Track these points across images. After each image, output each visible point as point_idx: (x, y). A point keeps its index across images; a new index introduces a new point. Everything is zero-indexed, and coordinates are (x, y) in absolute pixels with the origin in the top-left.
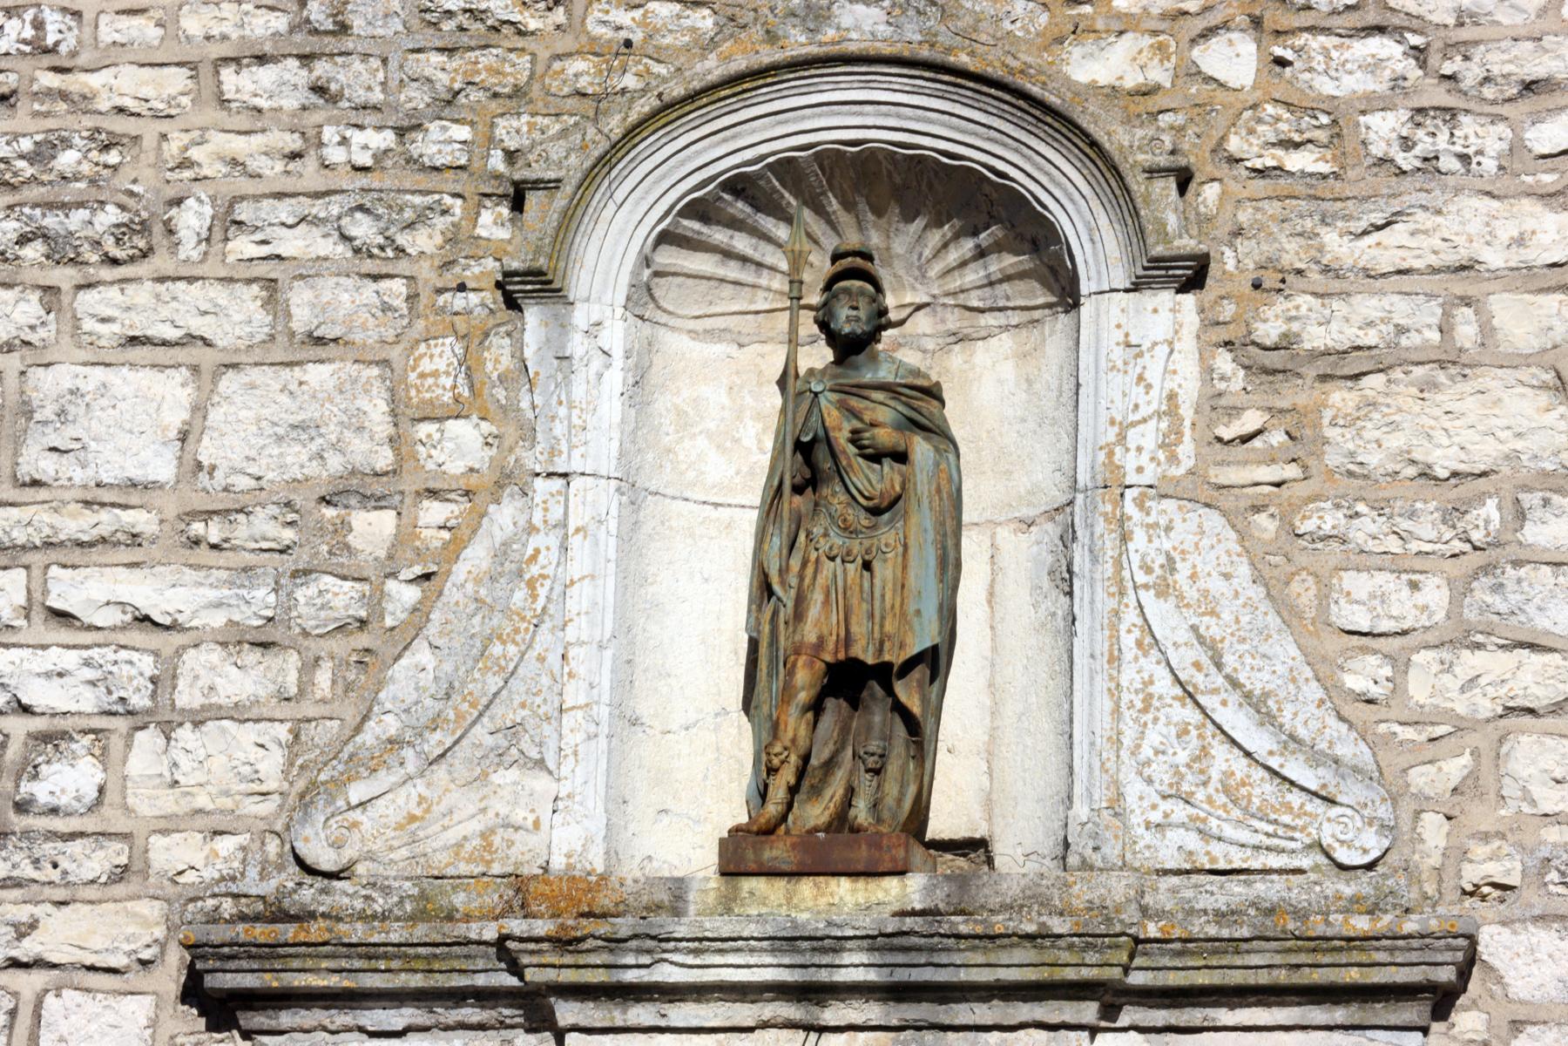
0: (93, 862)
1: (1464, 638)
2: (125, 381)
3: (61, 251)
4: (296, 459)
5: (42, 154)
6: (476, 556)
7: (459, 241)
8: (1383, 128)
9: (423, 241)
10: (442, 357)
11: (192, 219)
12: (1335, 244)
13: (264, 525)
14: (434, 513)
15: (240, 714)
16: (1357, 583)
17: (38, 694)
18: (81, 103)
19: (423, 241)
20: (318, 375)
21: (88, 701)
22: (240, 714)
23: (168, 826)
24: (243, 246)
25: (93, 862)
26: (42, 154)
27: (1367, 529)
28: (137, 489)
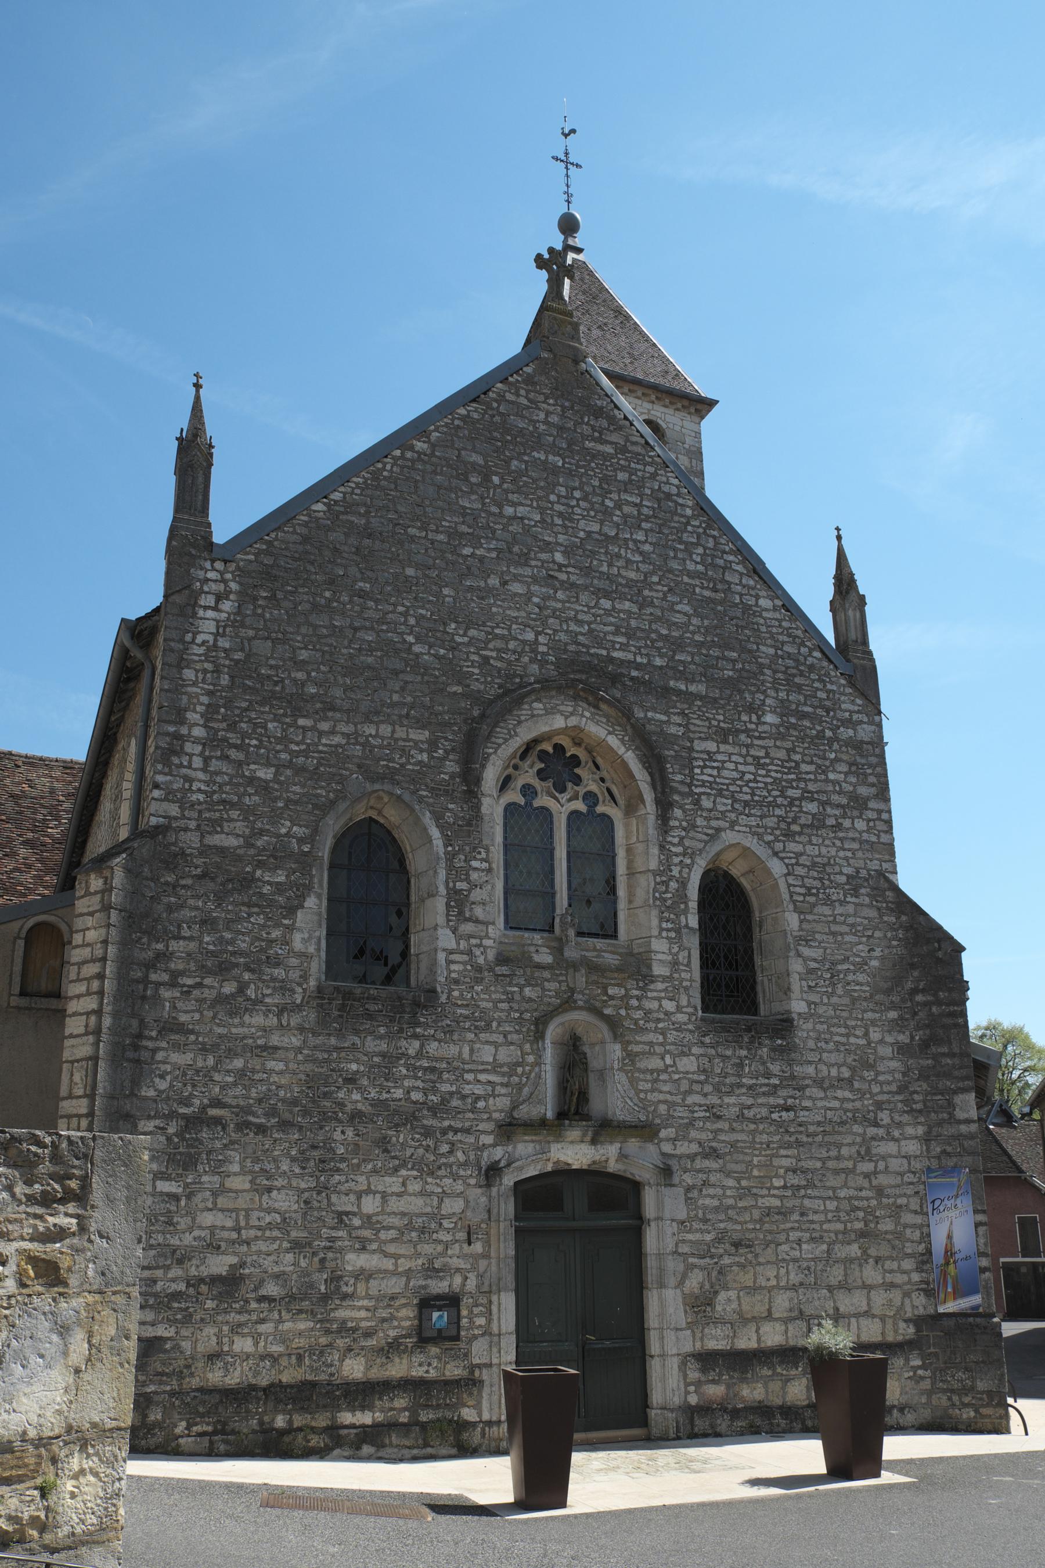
0: (485, 1116)
1: (653, 1090)
2: (487, 1047)
3: (476, 1027)
4: (509, 1060)
5: (473, 1013)
6: (533, 1075)
7: (529, 1029)
8: (641, 1022)
9: (524, 1030)
10: (527, 1046)
11: (494, 1024)
12: (637, 1038)
13: (505, 1069)
14: (527, 1068)
15: (504, 1095)
16: (641, 1083)
17: (476, 1092)
18: (478, 1006)
19: (524, 1030)
20: (512, 1047)
21: (483, 1093)
22: (504, 1095)
23: (495, 1111)
24: (501, 1029)
25: (485, 1116)
26: (473, 1013)
27: (642, 1076)
28: (487, 1063)
